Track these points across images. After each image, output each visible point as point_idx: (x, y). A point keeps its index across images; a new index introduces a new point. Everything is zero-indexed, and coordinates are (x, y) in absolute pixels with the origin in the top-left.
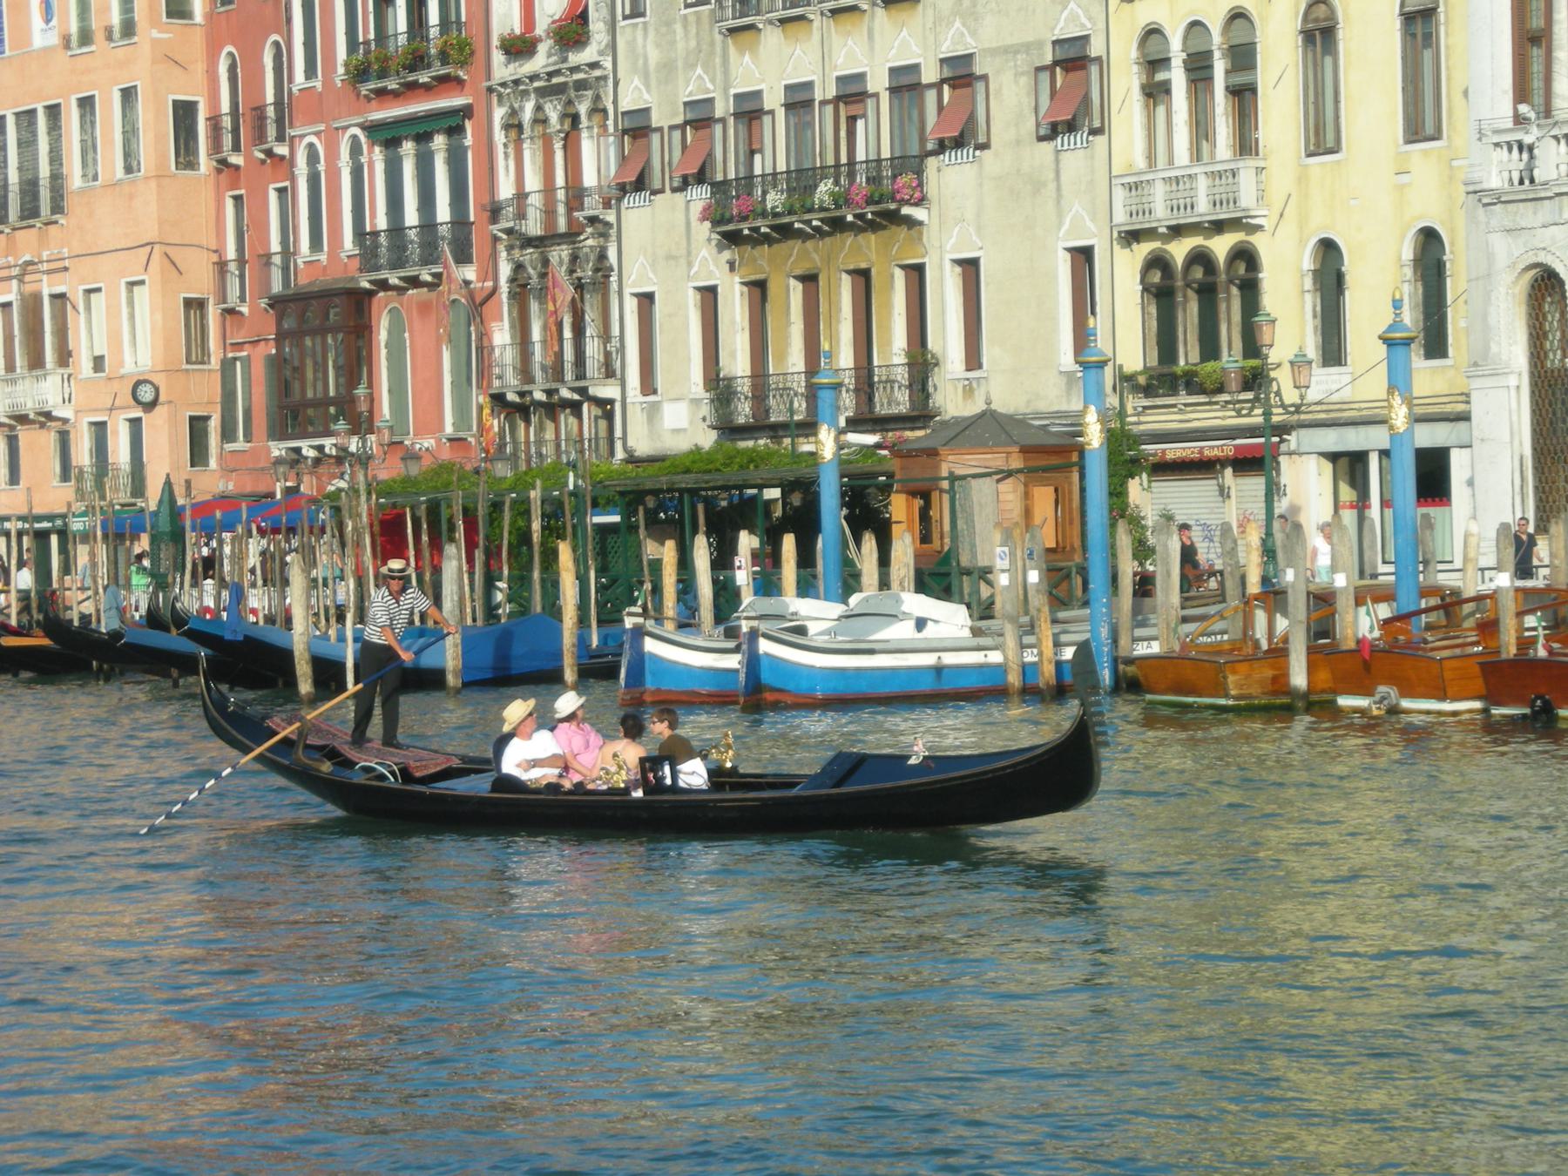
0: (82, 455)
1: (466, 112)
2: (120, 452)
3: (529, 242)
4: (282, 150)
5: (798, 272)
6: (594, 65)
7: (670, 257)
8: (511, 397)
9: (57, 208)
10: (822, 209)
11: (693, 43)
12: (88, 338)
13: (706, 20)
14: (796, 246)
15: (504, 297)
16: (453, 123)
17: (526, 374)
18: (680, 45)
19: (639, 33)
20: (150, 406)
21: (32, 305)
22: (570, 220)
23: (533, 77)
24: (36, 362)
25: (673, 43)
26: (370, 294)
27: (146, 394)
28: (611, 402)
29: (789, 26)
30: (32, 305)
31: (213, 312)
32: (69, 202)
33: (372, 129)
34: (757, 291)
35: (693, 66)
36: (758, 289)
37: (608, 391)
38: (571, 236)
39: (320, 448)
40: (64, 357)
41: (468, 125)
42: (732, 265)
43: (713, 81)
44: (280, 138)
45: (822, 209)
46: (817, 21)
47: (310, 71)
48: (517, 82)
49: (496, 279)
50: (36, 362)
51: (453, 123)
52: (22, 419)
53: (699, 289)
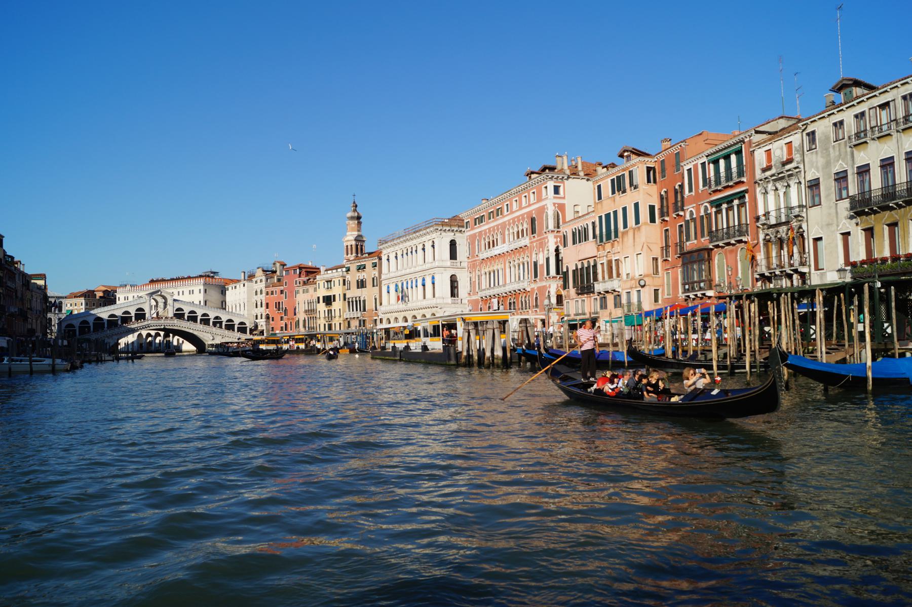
0: (624, 300)
1: (746, 191)
2: (634, 299)
3: (771, 226)
4: (681, 213)
5: (888, 222)
6: (797, 168)
7: (828, 225)
8: (767, 274)
9: (616, 236)
10: (903, 197)
11: (837, 153)
12: (625, 269)
13: (843, 146)
14: (887, 213)
15: (762, 245)
16: (741, 196)
17: (768, 268)
18: (832, 155)
19: (814, 156)
20: (643, 287)
21: (610, 262)
22: (787, 216)
23: (773, 175)
24: (611, 276)
25: (829, 155)
26: (712, 249)
27: (642, 283)
28: (805, 273)
29: (881, 140)
30: (610, 262)
31: (660, 261)
32: (620, 235)
33: (711, 202)
34: (869, 233)
35: (838, 161)
36: (869, 232)
37: (804, 270)
38: (787, 223)
39: (696, 295)
40: (618, 275)
41: (747, 195)
42: (857, 224)
43: (847, 164)
44: (683, 210)
45: (903, 197)
46: (895, 135)
47: (690, 190)
48: (766, 178)
49: (758, 239)
50: (611, 276)
51: (741, 196)
52: (607, 292)
53: (842, 234)
